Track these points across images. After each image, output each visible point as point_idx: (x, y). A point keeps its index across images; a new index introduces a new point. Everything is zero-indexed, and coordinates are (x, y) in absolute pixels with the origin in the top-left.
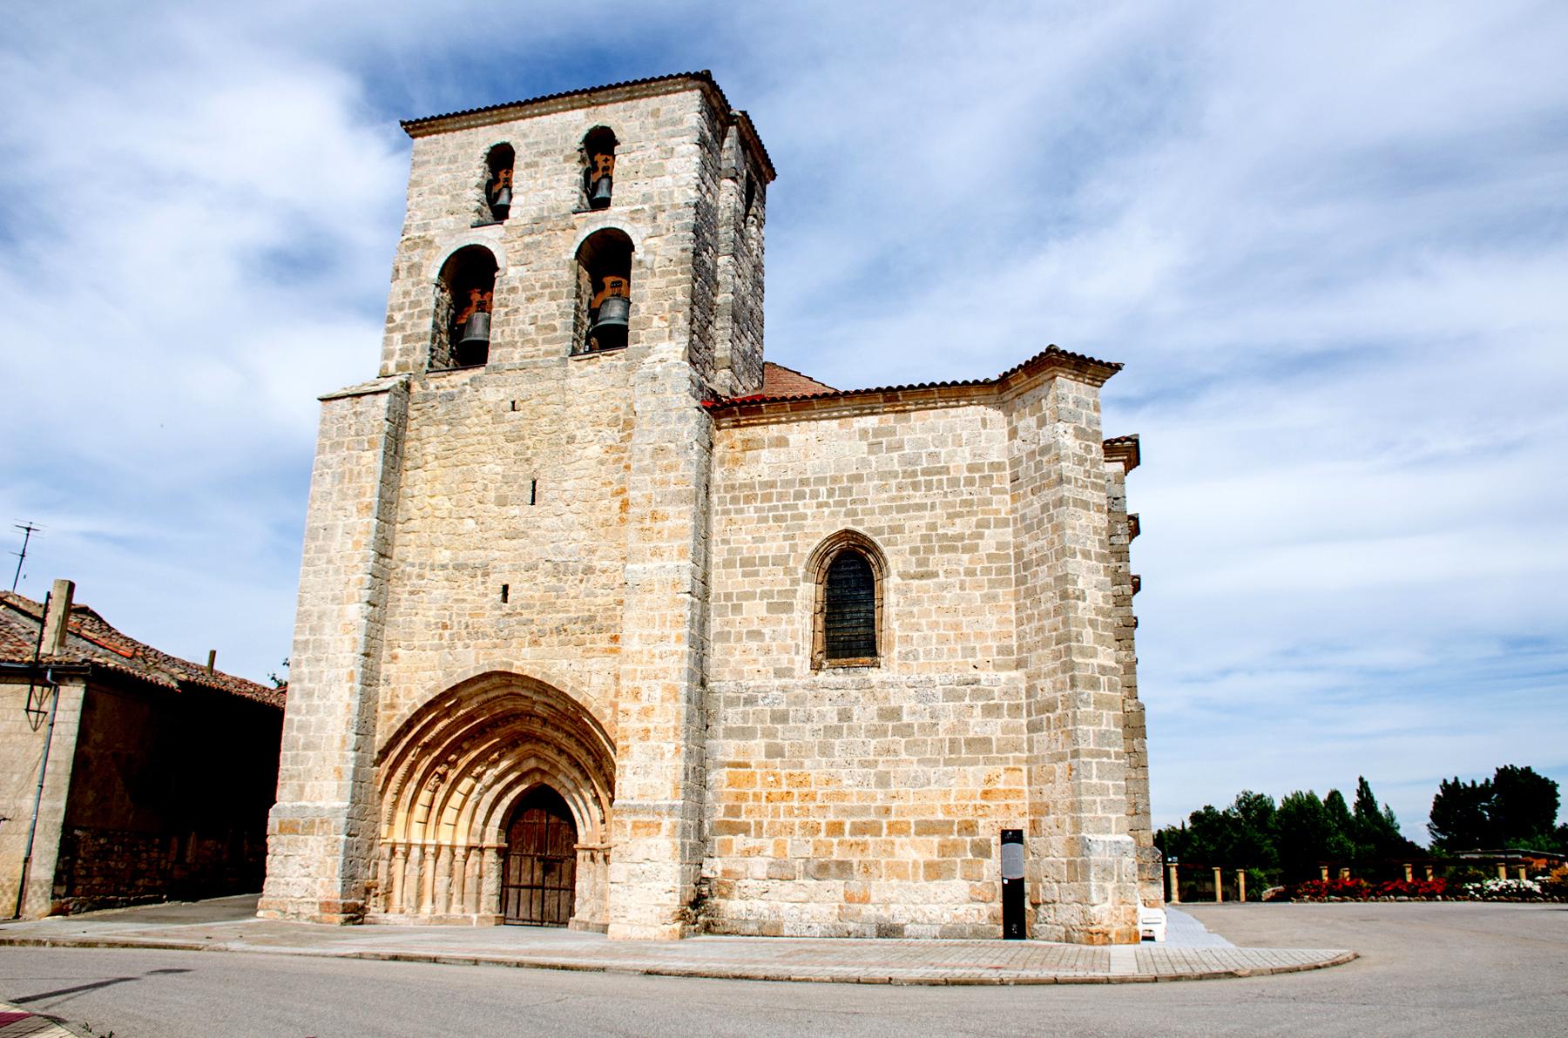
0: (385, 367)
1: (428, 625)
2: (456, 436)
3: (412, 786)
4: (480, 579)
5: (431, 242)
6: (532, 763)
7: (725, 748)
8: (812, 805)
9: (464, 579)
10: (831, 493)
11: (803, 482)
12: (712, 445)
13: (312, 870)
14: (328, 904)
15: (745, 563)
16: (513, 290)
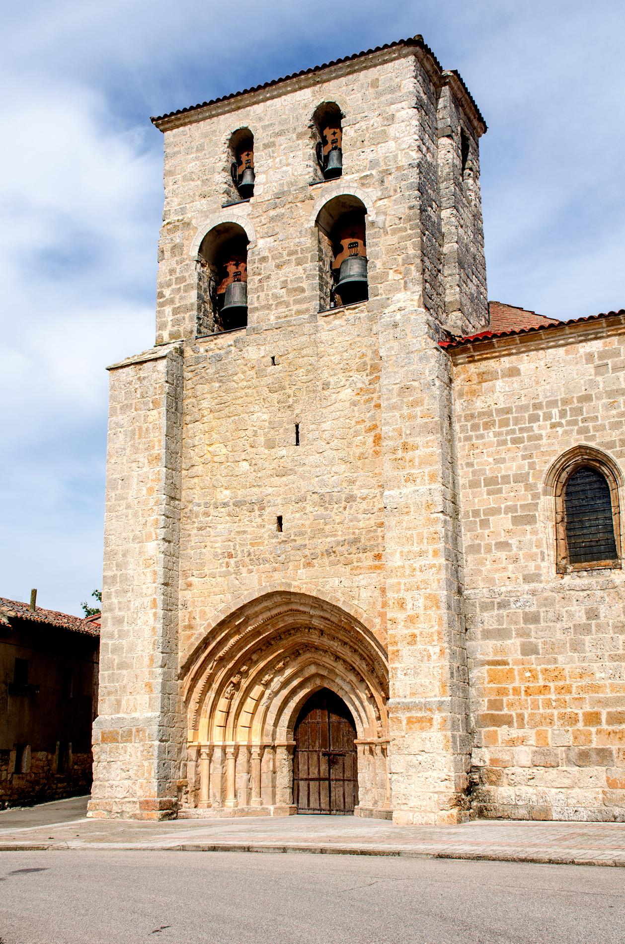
0: (160, 337)
1: (216, 555)
2: (227, 391)
3: (211, 695)
4: (257, 513)
5: (189, 224)
6: (313, 670)
7: (483, 648)
8: (568, 697)
9: (244, 512)
10: (563, 414)
11: (537, 406)
12: (451, 381)
13: (131, 773)
14: (147, 802)
15: (489, 482)
16: (264, 259)
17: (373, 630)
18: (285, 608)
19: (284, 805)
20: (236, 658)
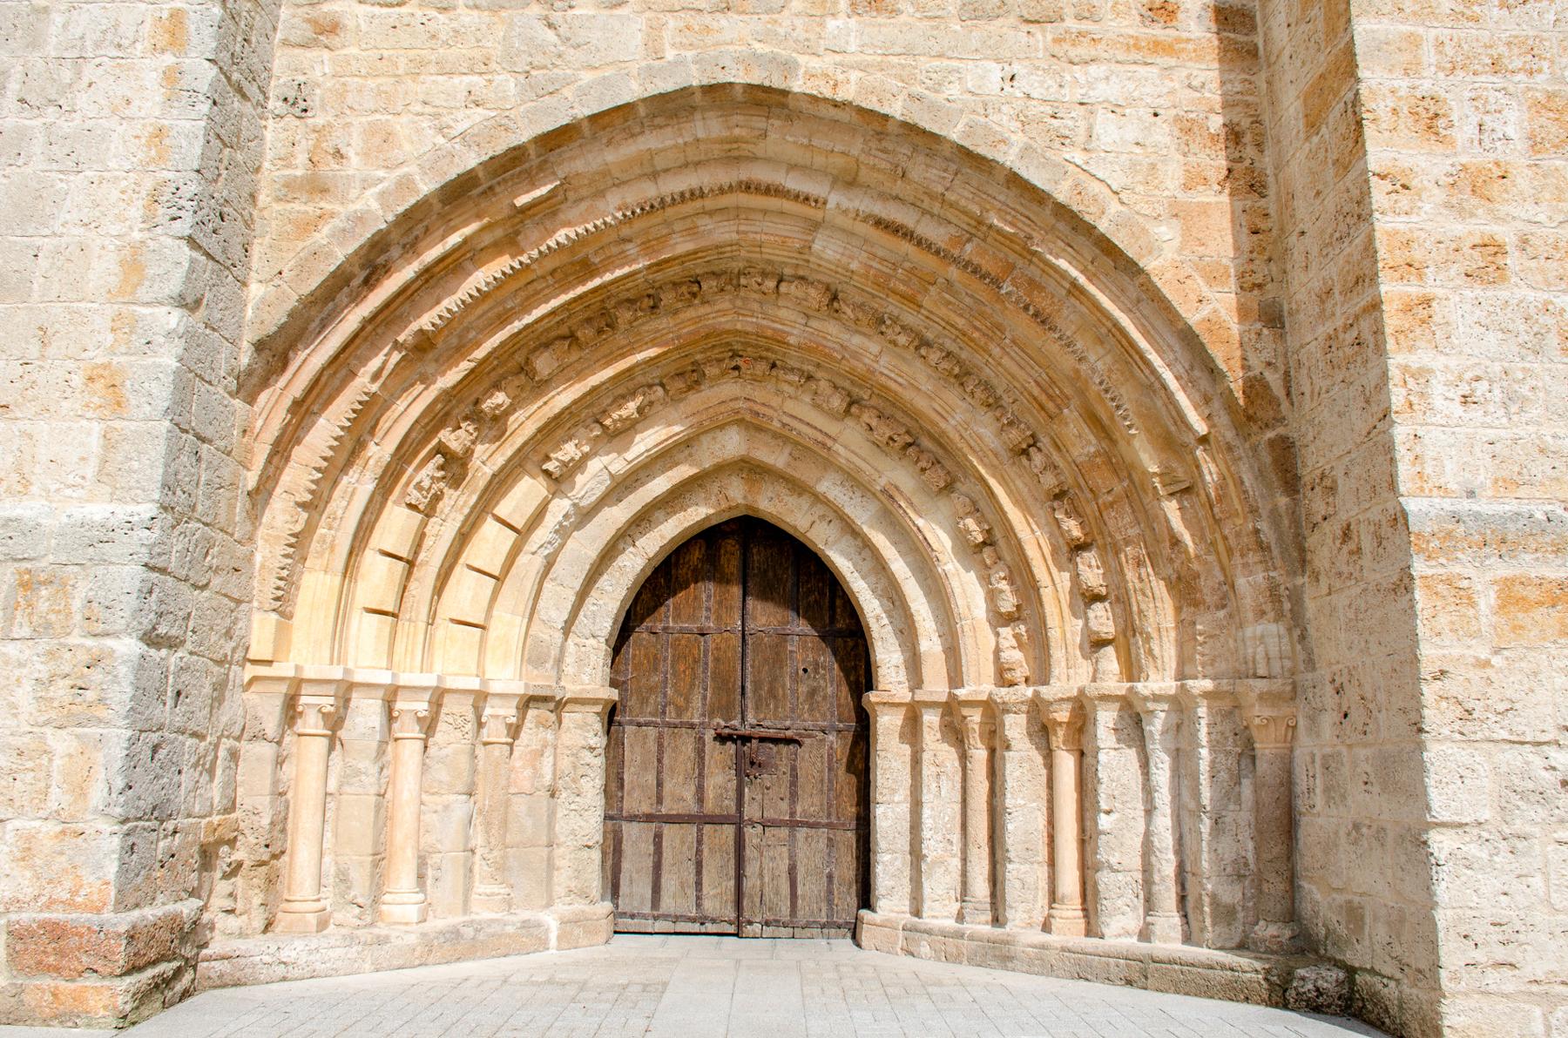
3: (359, 484)
6: (732, 444)
17: (1150, 264)
18: (725, 176)
19: (580, 906)
20: (480, 353)
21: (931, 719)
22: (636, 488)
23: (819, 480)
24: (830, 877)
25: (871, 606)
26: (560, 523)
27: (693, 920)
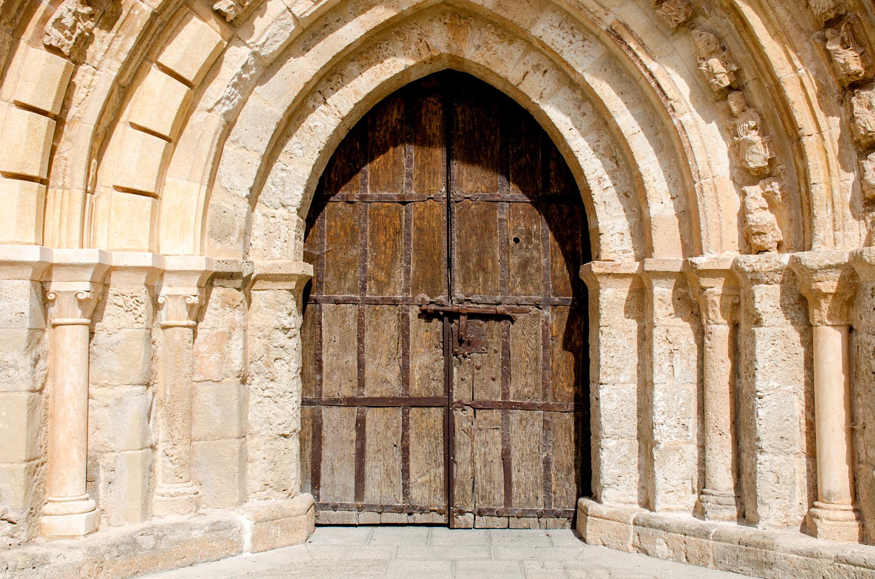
19: (278, 500)
21: (663, 291)
22: (324, 36)
23: (534, 22)
24: (547, 462)
25: (592, 167)
26: (239, 76)
27: (400, 510)
